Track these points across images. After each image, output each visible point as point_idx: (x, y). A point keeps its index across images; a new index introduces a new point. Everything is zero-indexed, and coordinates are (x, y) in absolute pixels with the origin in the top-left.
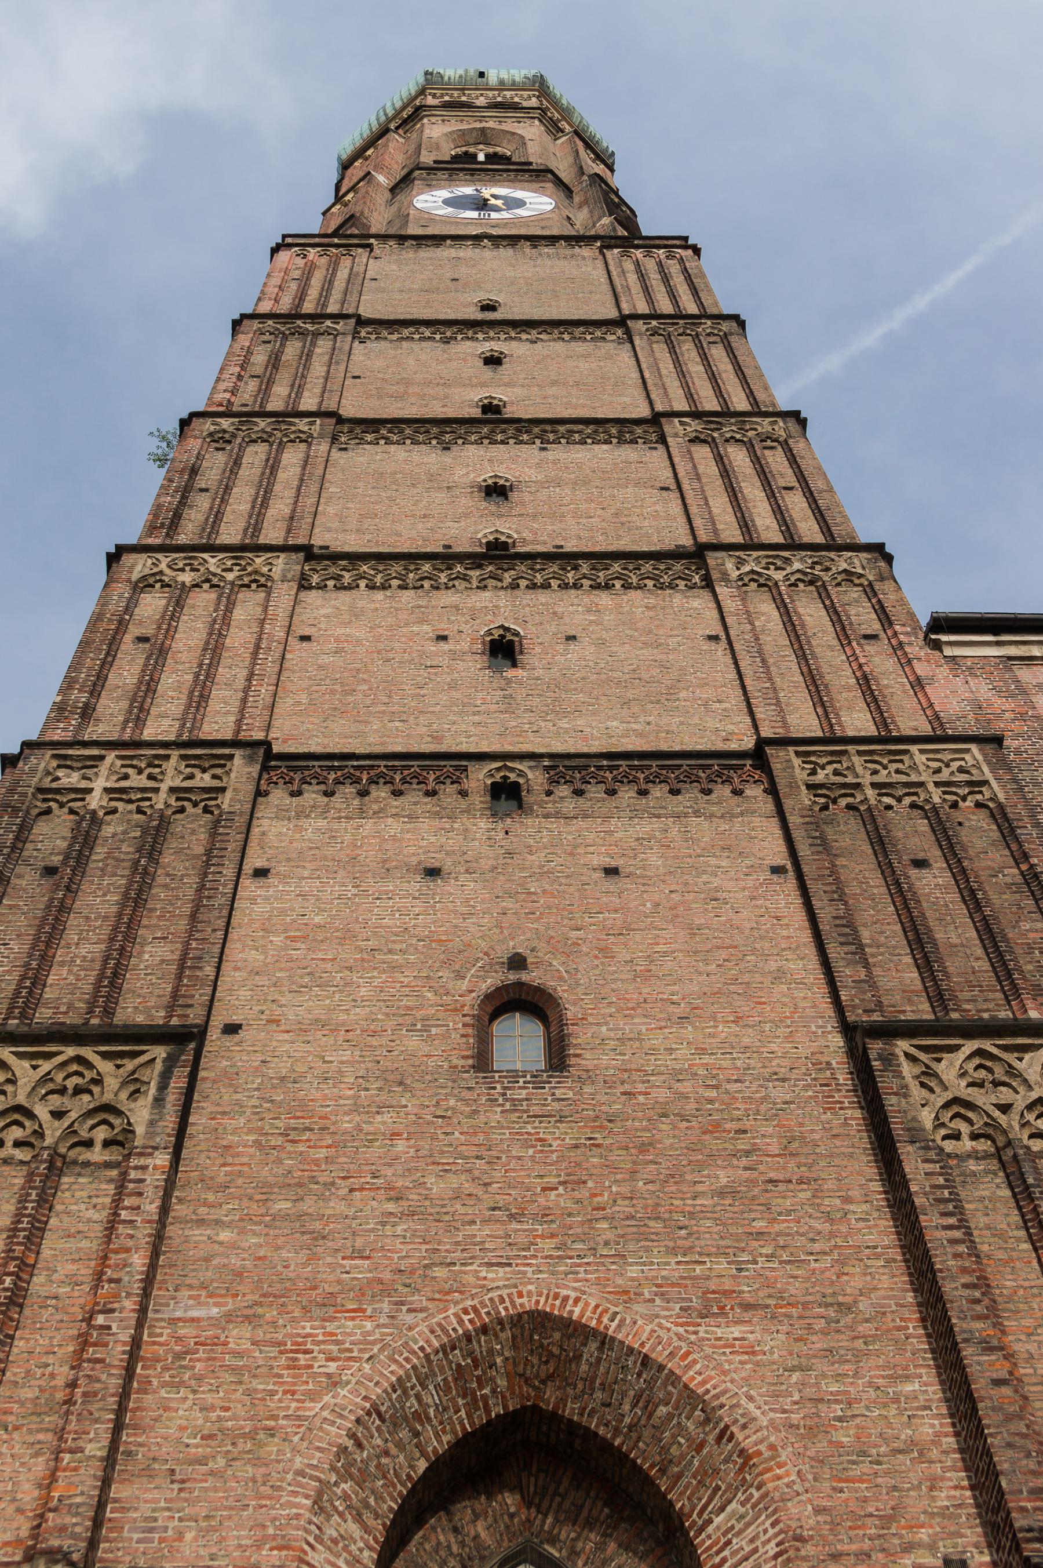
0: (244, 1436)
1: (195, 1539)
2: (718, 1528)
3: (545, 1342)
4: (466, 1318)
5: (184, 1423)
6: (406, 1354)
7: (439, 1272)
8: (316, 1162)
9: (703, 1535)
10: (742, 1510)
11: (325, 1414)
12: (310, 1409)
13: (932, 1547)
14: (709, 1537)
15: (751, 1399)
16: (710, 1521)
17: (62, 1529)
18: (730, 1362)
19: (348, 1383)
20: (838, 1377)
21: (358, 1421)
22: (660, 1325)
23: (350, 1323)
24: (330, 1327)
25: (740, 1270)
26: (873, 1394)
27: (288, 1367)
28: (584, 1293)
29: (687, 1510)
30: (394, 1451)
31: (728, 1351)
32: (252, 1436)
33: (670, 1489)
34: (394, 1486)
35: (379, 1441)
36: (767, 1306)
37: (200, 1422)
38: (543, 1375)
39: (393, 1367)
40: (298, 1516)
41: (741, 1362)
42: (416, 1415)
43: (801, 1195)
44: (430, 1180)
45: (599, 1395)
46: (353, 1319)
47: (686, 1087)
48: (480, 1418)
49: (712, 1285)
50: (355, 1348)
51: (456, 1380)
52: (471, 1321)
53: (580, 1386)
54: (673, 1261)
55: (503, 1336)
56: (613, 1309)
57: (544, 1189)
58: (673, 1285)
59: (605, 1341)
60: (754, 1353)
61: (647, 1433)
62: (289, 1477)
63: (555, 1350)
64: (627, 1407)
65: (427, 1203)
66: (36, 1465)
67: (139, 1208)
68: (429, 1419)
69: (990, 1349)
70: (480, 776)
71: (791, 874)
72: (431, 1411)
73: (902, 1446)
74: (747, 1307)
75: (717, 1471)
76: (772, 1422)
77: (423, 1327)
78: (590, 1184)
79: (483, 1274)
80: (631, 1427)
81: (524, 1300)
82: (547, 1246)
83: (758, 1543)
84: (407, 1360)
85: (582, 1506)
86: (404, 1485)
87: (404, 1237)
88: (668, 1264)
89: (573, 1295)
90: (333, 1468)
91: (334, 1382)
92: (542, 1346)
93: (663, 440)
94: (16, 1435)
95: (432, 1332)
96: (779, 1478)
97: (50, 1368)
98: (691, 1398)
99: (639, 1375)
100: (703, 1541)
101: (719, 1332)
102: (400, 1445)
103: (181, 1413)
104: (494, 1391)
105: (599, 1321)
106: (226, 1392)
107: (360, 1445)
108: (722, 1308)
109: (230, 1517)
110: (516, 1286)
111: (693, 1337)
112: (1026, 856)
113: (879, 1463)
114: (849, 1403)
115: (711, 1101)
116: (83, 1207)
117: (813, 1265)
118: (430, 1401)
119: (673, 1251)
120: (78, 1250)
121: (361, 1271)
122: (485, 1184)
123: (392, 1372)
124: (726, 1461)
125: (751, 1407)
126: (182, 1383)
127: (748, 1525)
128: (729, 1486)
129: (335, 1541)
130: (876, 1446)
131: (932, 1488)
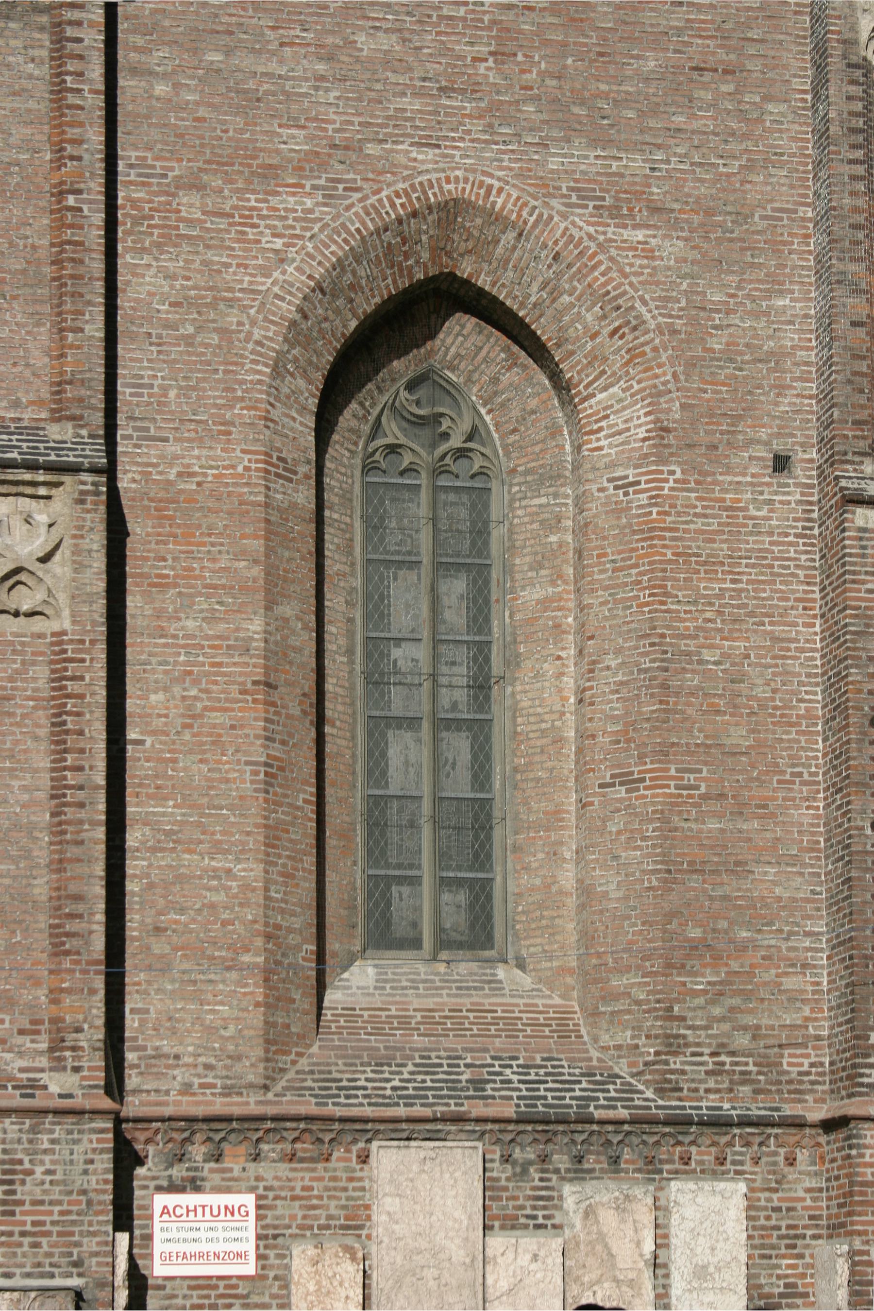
0: (206, 305)
1: (178, 396)
2: (599, 402)
3: (468, 224)
4: (398, 202)
5: (153, 289)
6: (344, 235)
7: (371, 149)
9: (586, 404)
10: (622, 395)
11: (276, 289)
12: (264, 284)
13: (767, 443)
14: (591, 407)
15: (645, 303)
16: (593, 395)
17: (81, 400)
18: (631, 265)
19: (294, 260)
21: (305, 298)
22: (573, 223)
23: (291, 199)
24: (274, 201)
25: (653, 169)
27: (238, 241)
28: (507, 183)
29: (575, 381)
30: (332, 316)
31: (631, 254)
32: (213, 305)
33: (562, 360)
34: (331, 343)
35: (320, 311)
36: (672, 211)
37: (166, 289)
38: (462, 250)
39: (333, 248)
40: (260, 382)
41: (641, 266)
42: (352, 287)
43: (724, 88)
45: (510, 274)
46: (294, 194)
48: (404, 283)
50: (298, 225)
51: (385, 255)
52: (402, 205)
53: (495, 264)
54: (592, 154)
55: (430, 219)
56: (534, 203)
57: (474, 59)
58: (589, 181)
60: (653, 258)
61: (549, 312)
62: (250, 346)
63: (476, 233)
64: (535, 288)
65: (358, 67)
66: (40, 334)
68: (361, 288)
72: (363, 282)
73: (763, 357)
76: (659, 326)
77: (358, 208)
78: (520, 58)
79: (414, 155)
80: (535, 305)
81: (451, 187)
83: (631, 425)
84: (345, 241)
86: (338, 341)
87: (337, 106)
88: (586, 157)
89: (497, 184)
90: (286, 340)
92: (464, 227)
94: (15, 305)
95: (368, 214)
96: (657, 376)
97: (30, 241)
99: (550, 266)
100: (585, 409)
102: (337, 312)
103: (147, 279)
104: (417, 262)
105: (519, 215)
106: (186, 261)
107: (305, 317)
108: (631, 209)
109: (204, 379)
110: (444, 171)
111: (601, 238)
113: (741, 370)
114: (727, 313)
117: (722, 169)
118: (363, 274)
122: (416, 48)
124: (615, 353)
125: (643, 310)
126: (144, 250)
127: (624, 408)
128: (614, 374)
129: (288, 397)
130: (742, 354)
131: (778, 395)
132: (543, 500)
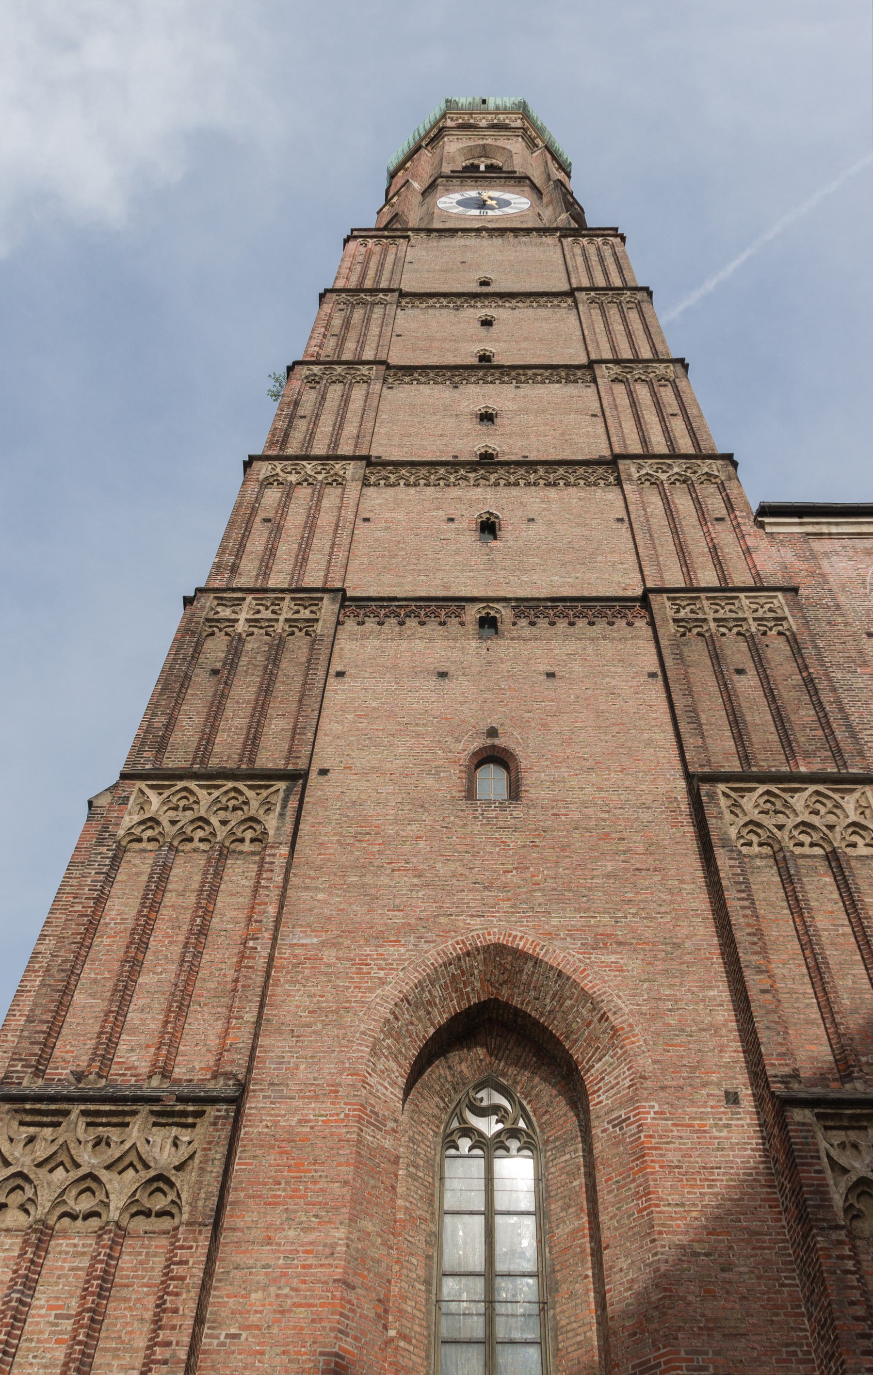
0: (332, 1012)
1: (306, 1069)
2: (597, 1070)
3: (503, 962)
4: (458, 947)
5: (299, 1004)
6: (423, 967)
7: (443, 920)
8: (373, 854)
9: (589, 1074)
10: (611, 1060)
11: (378, 1000)
12: (369, 997)
13: (718, 1085)
14: (592, 1075)
15: (619, 997)
16: (593, 1066)
17: (233, 1061)
18: (608, 976)
19: (390, 983)
20: (670, 986)
21: (396, 1004)
22: (569, 953)
23: (392, 949)
24: (381, 950)
25: (617, 922)
26: (690, 996)
27: (357, 973)
28: (526, 933)
29: (580, 1060)
30: (416, 1022)
31: (607, 969)
33: (570, 1048)
34: (416, 1042)
35: (407, 1016)
36: (632, 944)
37: (308, 1003)
38: (501, 981)
39: (416, 974)
40: (362, 1058)
41: (615, 976)
42: (429, 1002)
43: (655, 878)
44: (439, 865)
45: (532, 993)
46: (393, 946)
47: (590, 811)
48: (465, 1005)
49: (600, 930)
50: (395, 963)
51: (451, 982)
52: (460, 949)
53: (522, 988)
54: (578, 916)
55: (479, 957)
56: (543, 943)
57: (504, 872)
58: (577, 930)
59: (537, 962)
60: (622, 971)
61: (559, 1015)
62: (358, 1035)
63: (509, 967)
64: (548, 1000)
65: (437, 879)
66: (217, 1025)
67: (271, 879)
68: (436, 1004)
69: (760, 972)
70: (473, 612)
71: (660, 678)
72: (437, 1000)
73: (705, 1027)
74: (620, 944)
75: (598, 1038)
76: (631, 1011)
77: (433, 952)
78: (531, 869)
79: (468, 921)
80: (550, 1012)
81: (491, 937)
82: (506, 905)
83: (620, 1079)
84: (424, 970)
85: (521, 1056)
86: (421, 1041)
87: (423, 899)
88: (575, 917)
89: (519, 934)
90: (382, 1031)
91: (383, 982)
92: (501, 964)
93: (595, 381)
94: (205, 1009)
95: (439, 954)
96: (633, 1043)
97: (223, 971)
98: (585, 996)
99: (556, 982)
100: (589, 1077)
101: (603, 958)
102: (419, 1019)
103: (297, 998)
104: (473, 989)
105: (534, 950)
106: (322, 986)
107: (397, 1018)
108: (605, 944)
109: (324, 1057)
110: (487, 929)
111: (588, 961)
112: (806, 667)
113: (691, 1036)
114: (676, 1001)
115: (604, 820)
116: (239, 878)
117: (660, 920)
118: (436, 994)
119: (578, 910)
120: (238, 903)
121: (398, 918)
122: (470, 868)
123: (415, 977)
124: (603, 1033)
125: (619, 1002)
126: (297, 981)
127: (614, 1069)
128: (605, 1047)
129: (383, 1072)
130: (691, 1026)
131: (721, 1051)
132: (568, 1157)
